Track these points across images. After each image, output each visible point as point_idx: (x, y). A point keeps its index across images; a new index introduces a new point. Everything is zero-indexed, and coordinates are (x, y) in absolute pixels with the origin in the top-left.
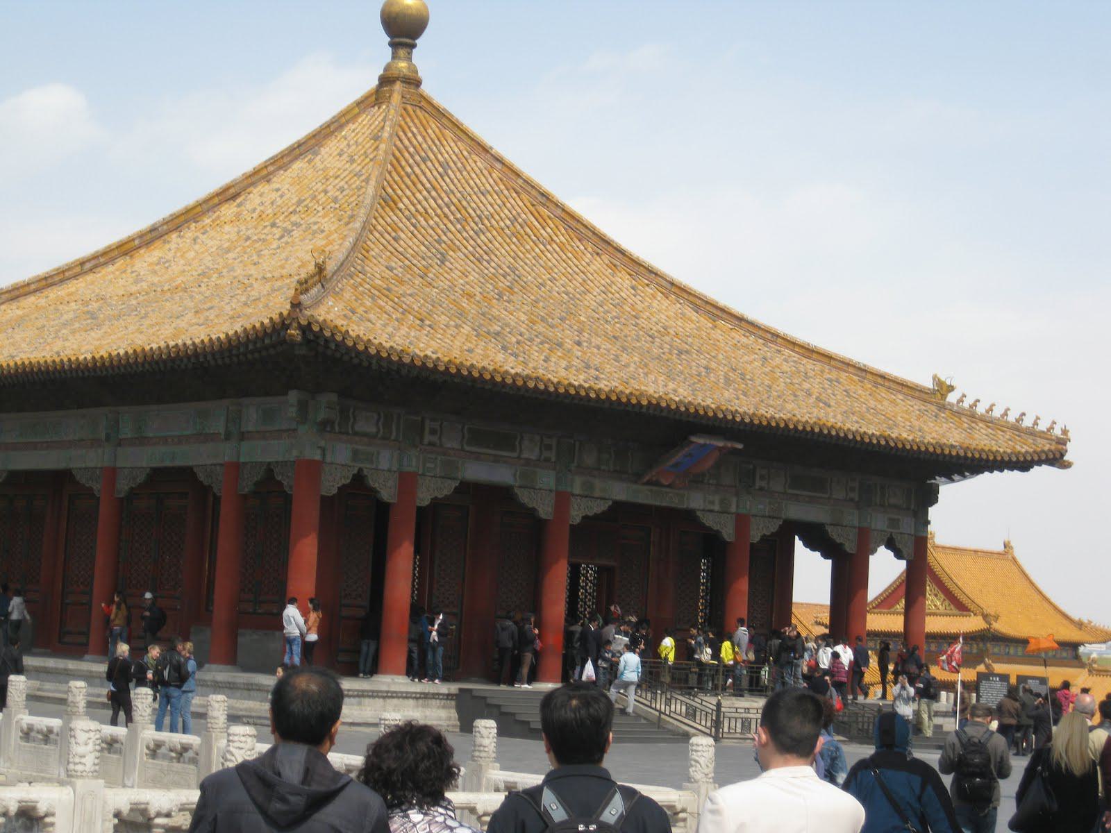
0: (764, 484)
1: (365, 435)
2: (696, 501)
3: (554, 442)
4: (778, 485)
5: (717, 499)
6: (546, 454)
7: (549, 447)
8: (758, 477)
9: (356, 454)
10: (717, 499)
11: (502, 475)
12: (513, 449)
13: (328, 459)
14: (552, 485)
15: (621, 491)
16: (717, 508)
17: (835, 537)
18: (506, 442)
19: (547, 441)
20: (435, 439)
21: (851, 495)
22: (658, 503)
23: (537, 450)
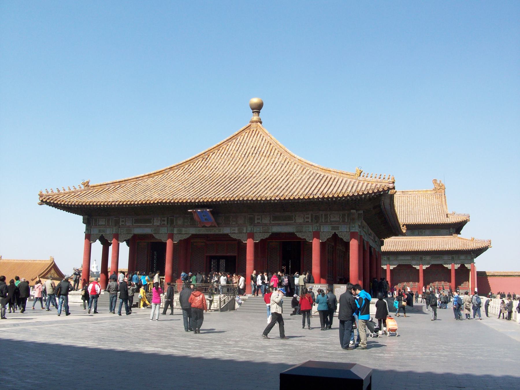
0: (259, 221)
1: (101, 225)
2: (226, 230)
3: (166, 219)
4: (266, 221)
5: (236, 229)
6: (163, 223)
7: (164, 221)
8: (256, 219)
9: (100, 231)
10: (236, 229)
11: (147, 231)
12: (150, 223)
13: (92, 233)
14: (166, 232)
15: (193, 231)
16: (236, 232)
17: (300, 236)
18: (148, 221)
19: (163, 219)
20: (123, 223)
21: (307, 220)
22: (209, 233)
23: (159, 222)
